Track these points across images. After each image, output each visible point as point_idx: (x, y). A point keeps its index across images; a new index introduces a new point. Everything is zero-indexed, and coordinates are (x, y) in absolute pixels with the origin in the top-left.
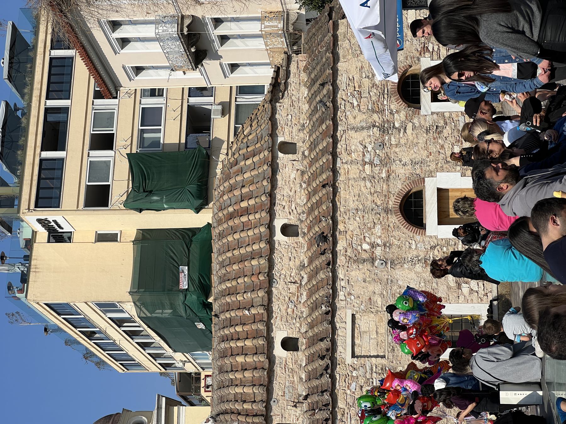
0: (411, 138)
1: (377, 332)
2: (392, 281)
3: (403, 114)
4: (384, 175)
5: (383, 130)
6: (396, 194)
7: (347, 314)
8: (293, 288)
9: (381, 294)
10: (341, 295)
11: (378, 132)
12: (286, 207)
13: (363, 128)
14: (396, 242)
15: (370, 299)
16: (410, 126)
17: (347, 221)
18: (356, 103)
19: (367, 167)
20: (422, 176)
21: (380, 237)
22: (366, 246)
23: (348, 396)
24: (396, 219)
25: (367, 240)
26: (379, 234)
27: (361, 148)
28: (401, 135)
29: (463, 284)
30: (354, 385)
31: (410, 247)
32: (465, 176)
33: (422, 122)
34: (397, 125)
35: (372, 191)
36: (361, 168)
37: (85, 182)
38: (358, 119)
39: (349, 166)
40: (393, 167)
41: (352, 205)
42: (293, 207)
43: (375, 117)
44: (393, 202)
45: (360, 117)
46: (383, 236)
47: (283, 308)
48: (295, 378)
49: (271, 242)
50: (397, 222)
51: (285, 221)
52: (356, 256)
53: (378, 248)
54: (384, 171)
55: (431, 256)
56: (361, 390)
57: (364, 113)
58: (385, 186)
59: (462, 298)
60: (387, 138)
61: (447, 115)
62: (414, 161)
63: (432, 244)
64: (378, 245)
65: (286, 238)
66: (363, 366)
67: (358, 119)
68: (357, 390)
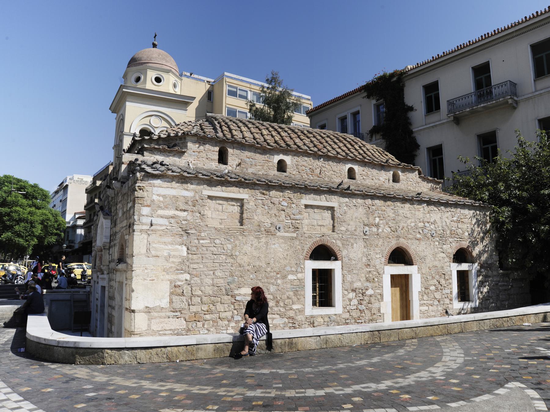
0: (438, 256)
1: (321, 226)
2: (356, 239)
3: (450, 251)
4: (418, 236)
5: (442, 237)
6: (408, 244)
7: (334, 203)
8: (318, 171)
9: (347, 230)
10: (347, 200)
11: (440, 233)
12: (364, 173)
13: (442, 222)
14: (380, 243)
15: (345, 222)
16: (444, 255)
17: (391, 207)
18: (455, 219)
19: (421, 225)
20: (418, 263)
21: (383, 231)
22: (377, 220)
23: (278, 199)
24: (393, 244)
25: (381, 222)
26: (385, 231)
27: (432, 221)
28: (439, 249)
29: (354, 294)
30: (285, 204)
31: (377, 254)
32: (419, 294)
33: (446, 264)
34: (444, 246)
35: (409, 227)
36: (421, 220)
37: (239, 109)
38: (447, 220)
39: (422, 211)
40: (423, 243)
41: (401, 211)
42: (365, 177)
43: (448, 232)
44: (404, 243)
45: (448, 222)
46: (383, 233)
47: (305, 163)
48: (259, 167)
49: (345, 160)
50: (392, 244)
51: (357, 171)
52: (371, 212)
53: (376, 229)
54: (420, 236)
55: (372, 269)
56: (282, 210)
57: (450, 224)
58: (412, 236)
59: (346, 292)
60: (438, 239)
61: (450, 281)
62: (426, 258)
63: (379, 270)
64: (378, 230)
65: (347, 170)
66: (300, 213)
67: (447, 220)
68: (282, 207)
